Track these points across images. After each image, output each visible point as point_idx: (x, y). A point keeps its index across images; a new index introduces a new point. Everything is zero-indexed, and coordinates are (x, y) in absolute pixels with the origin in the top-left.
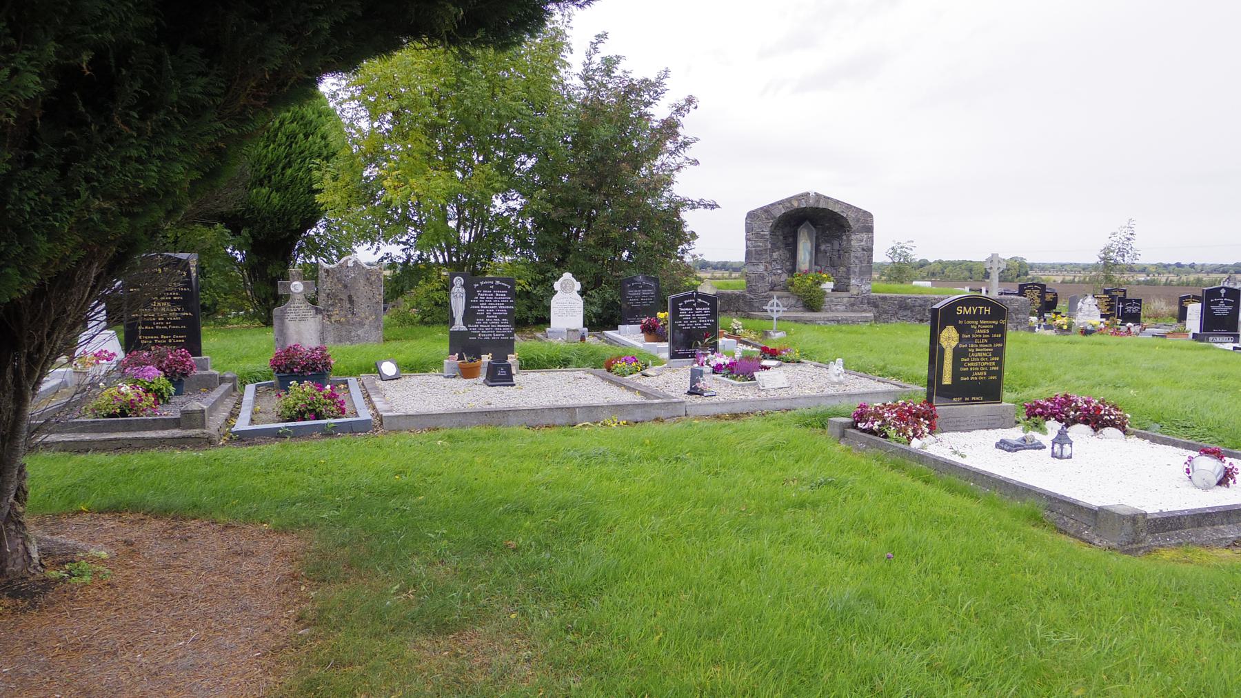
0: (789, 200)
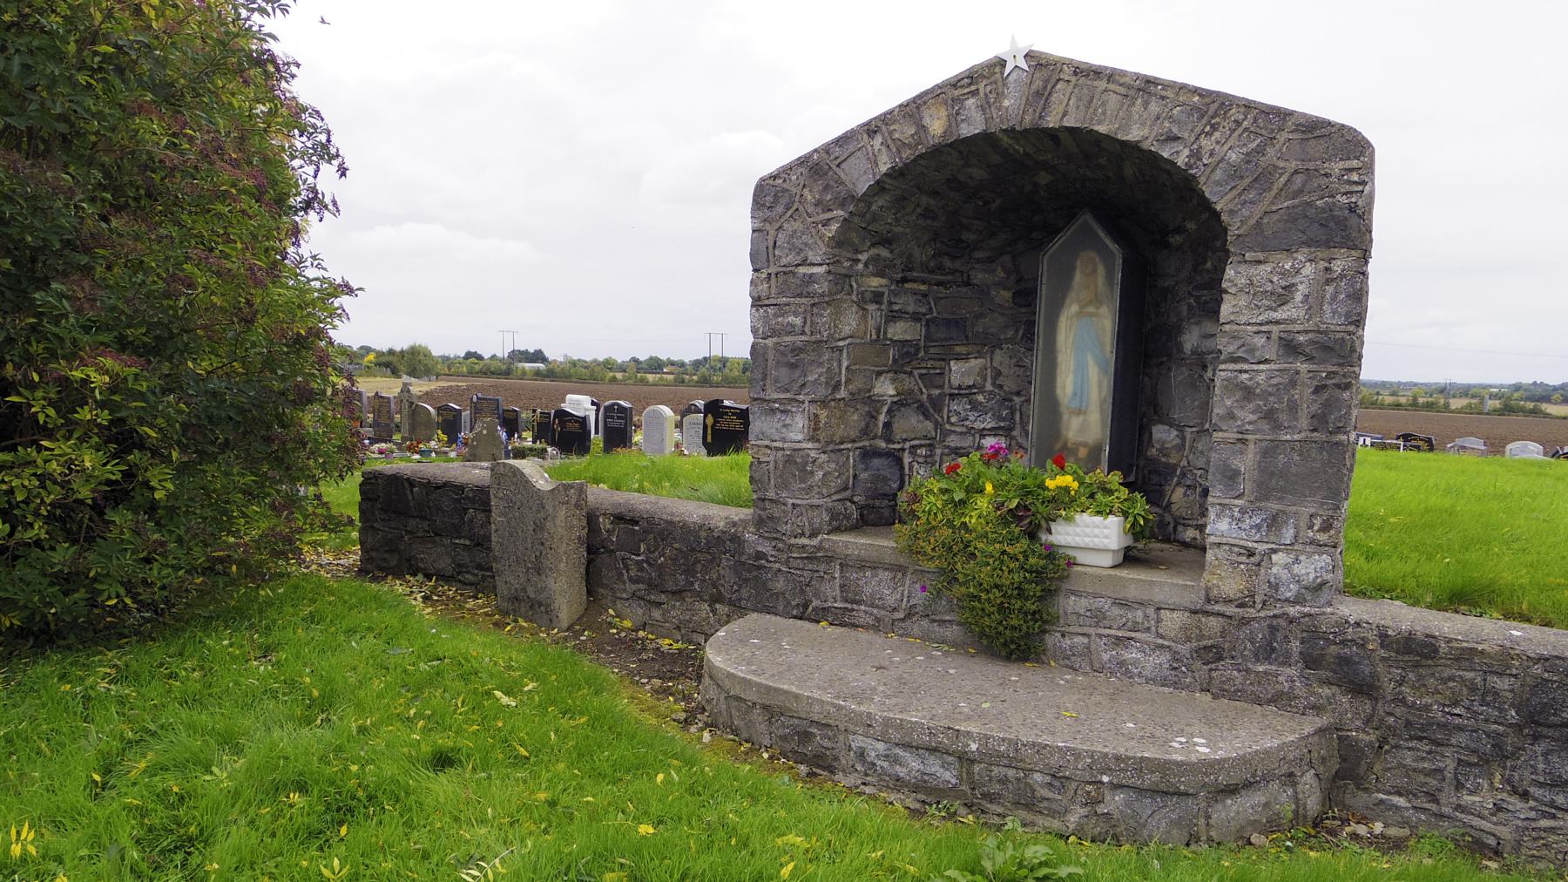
0: (913, 109)
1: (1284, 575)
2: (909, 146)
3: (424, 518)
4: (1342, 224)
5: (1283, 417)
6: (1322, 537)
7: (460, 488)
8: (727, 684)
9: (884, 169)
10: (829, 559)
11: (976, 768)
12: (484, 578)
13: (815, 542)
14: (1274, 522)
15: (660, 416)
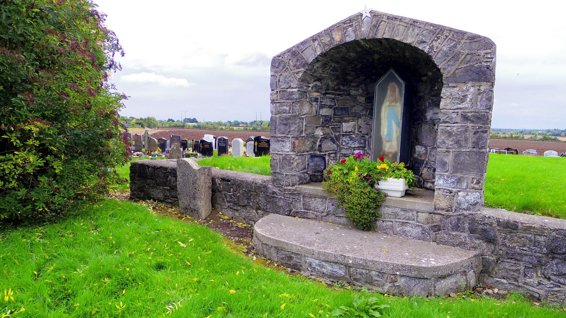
0: (329, 32)
1: (463, 200)
2: (327, 45)
3: (153, 179)
4: (484, 73)
5: (463, 143)
6: (477, 186)
7: (166, 169)
8: (262, 239)
9: (318, 53)
10: (299, 194)
11: (352, 269)
12: (175, 201)
13: (294, 188)
14: (459, 181)
15: (238, 143)
